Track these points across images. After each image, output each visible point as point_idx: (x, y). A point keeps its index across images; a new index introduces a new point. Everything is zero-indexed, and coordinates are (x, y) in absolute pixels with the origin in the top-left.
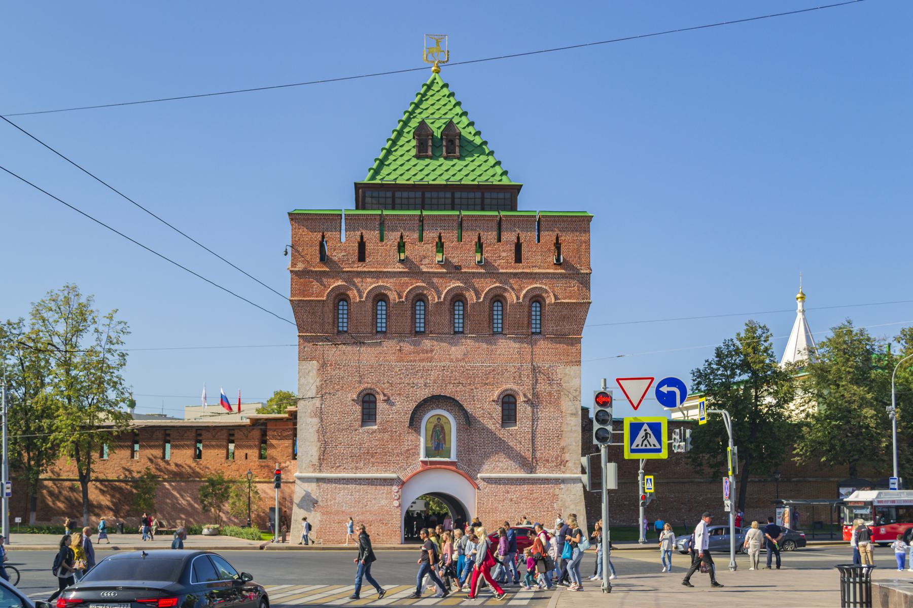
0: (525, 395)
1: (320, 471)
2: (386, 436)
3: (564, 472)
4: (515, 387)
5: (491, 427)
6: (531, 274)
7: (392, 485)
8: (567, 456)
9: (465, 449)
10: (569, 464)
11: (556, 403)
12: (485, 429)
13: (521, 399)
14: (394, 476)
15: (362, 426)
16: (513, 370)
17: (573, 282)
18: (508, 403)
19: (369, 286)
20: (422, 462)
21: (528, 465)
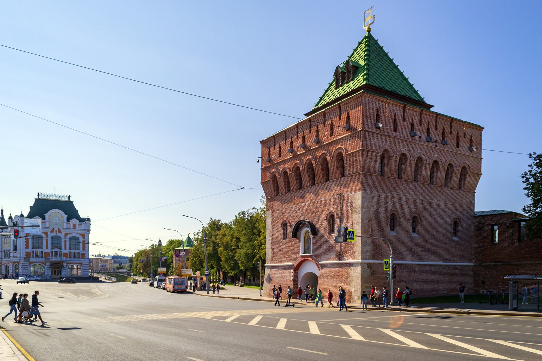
0: (337, 214)
1: (272, 263)
2: (290, 244)
3: (353, 259)
4: (333, 210)
5: (325, 235)
6: (336, 140)
7: (290, 270)
8: (355, 249)
9: (316, 249)
10: (356, 254)
11: (350, 217)
12: (323, 236)
13: (336, 217)
14: (291, 264)
15: (284, 239)
16: (333, 200)
17: (355, 139)
18: (331, 218)
19: (281, 168)
20: (301, 256)
21: (340, 256)
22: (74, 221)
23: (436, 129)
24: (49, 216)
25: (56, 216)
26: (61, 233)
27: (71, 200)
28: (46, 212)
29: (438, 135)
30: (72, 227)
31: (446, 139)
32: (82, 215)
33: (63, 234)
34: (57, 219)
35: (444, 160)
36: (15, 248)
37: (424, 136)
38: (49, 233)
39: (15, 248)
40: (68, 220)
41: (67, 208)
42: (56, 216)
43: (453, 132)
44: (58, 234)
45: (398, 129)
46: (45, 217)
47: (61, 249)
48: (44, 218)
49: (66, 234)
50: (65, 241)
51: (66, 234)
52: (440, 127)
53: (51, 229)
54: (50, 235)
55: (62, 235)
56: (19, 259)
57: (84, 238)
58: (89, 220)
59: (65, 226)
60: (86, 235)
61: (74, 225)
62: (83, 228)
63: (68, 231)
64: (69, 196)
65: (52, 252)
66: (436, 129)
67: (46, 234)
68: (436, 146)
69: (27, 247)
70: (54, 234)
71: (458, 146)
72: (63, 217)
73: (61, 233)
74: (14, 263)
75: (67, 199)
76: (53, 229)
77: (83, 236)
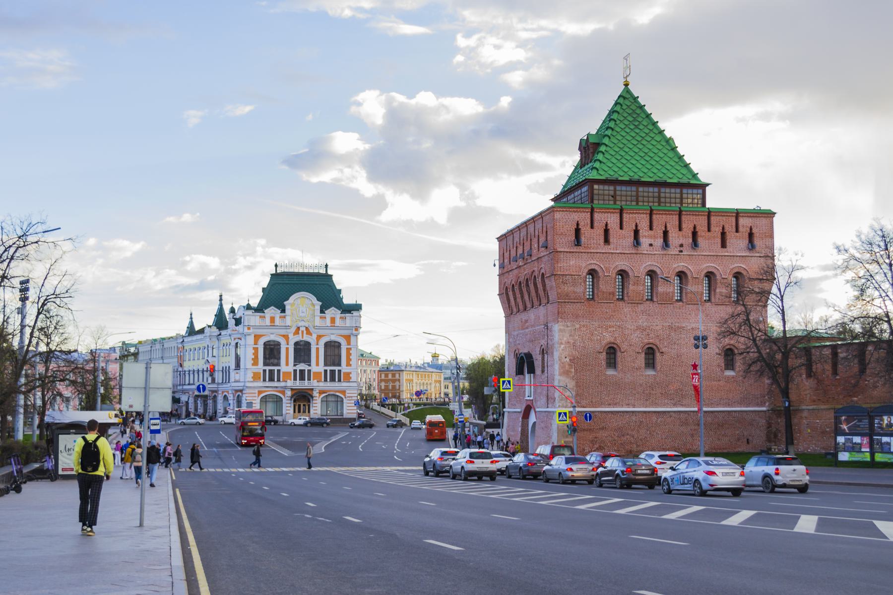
22: (332, 312)
23: (680, 229)
24: (292, 305)
25: (302, 304)
26: (311, 334)
27: (330, 272)
28: (287, 299)
29: (685, 237)
30: (328, 323)
31: (700, 240)
32: (347, 300)
33: (315, 336)
34: (304, 310)
35: (696, 267)
36: (238, 366)
37: (660, 241)
38: (291, 336)
39: (238, 366)
40: (322, 312)
41: (321, 287)
42: (302, 304)
43: (713, 228)
44: (306, 338)
45: (611, 240)
46: (284, 306)
47: (310, 365)
48: (283, 311)
49: (319, 337)
50: (317, 349)
51: (319, 337)
52: (687, 227)
53: (293, 329)
54: (293, 339)
55: (312, 339)
56: (242, 384)
57: (349, 344)
58: (357, 307)
59: (318, 322)
60: (353, 339)
61: (333, 320)
62: (348, 325)
63: (321, 332)
64: (326, 266)
65: (295, 371)
66: (680, 229)
67: (286, 337)
68: (681, 251)
69: (255, 363)
70: (298, 338)
71: (724, 245)
72: (313, 305)
73: (311, 334)
74: (237, 391)
75: (323, 271)
76: (298, 328)
77: (348, 338)
